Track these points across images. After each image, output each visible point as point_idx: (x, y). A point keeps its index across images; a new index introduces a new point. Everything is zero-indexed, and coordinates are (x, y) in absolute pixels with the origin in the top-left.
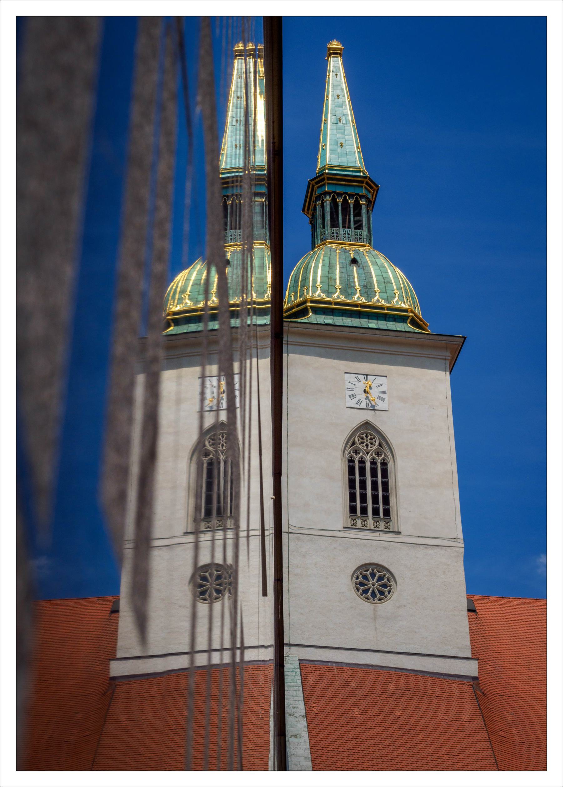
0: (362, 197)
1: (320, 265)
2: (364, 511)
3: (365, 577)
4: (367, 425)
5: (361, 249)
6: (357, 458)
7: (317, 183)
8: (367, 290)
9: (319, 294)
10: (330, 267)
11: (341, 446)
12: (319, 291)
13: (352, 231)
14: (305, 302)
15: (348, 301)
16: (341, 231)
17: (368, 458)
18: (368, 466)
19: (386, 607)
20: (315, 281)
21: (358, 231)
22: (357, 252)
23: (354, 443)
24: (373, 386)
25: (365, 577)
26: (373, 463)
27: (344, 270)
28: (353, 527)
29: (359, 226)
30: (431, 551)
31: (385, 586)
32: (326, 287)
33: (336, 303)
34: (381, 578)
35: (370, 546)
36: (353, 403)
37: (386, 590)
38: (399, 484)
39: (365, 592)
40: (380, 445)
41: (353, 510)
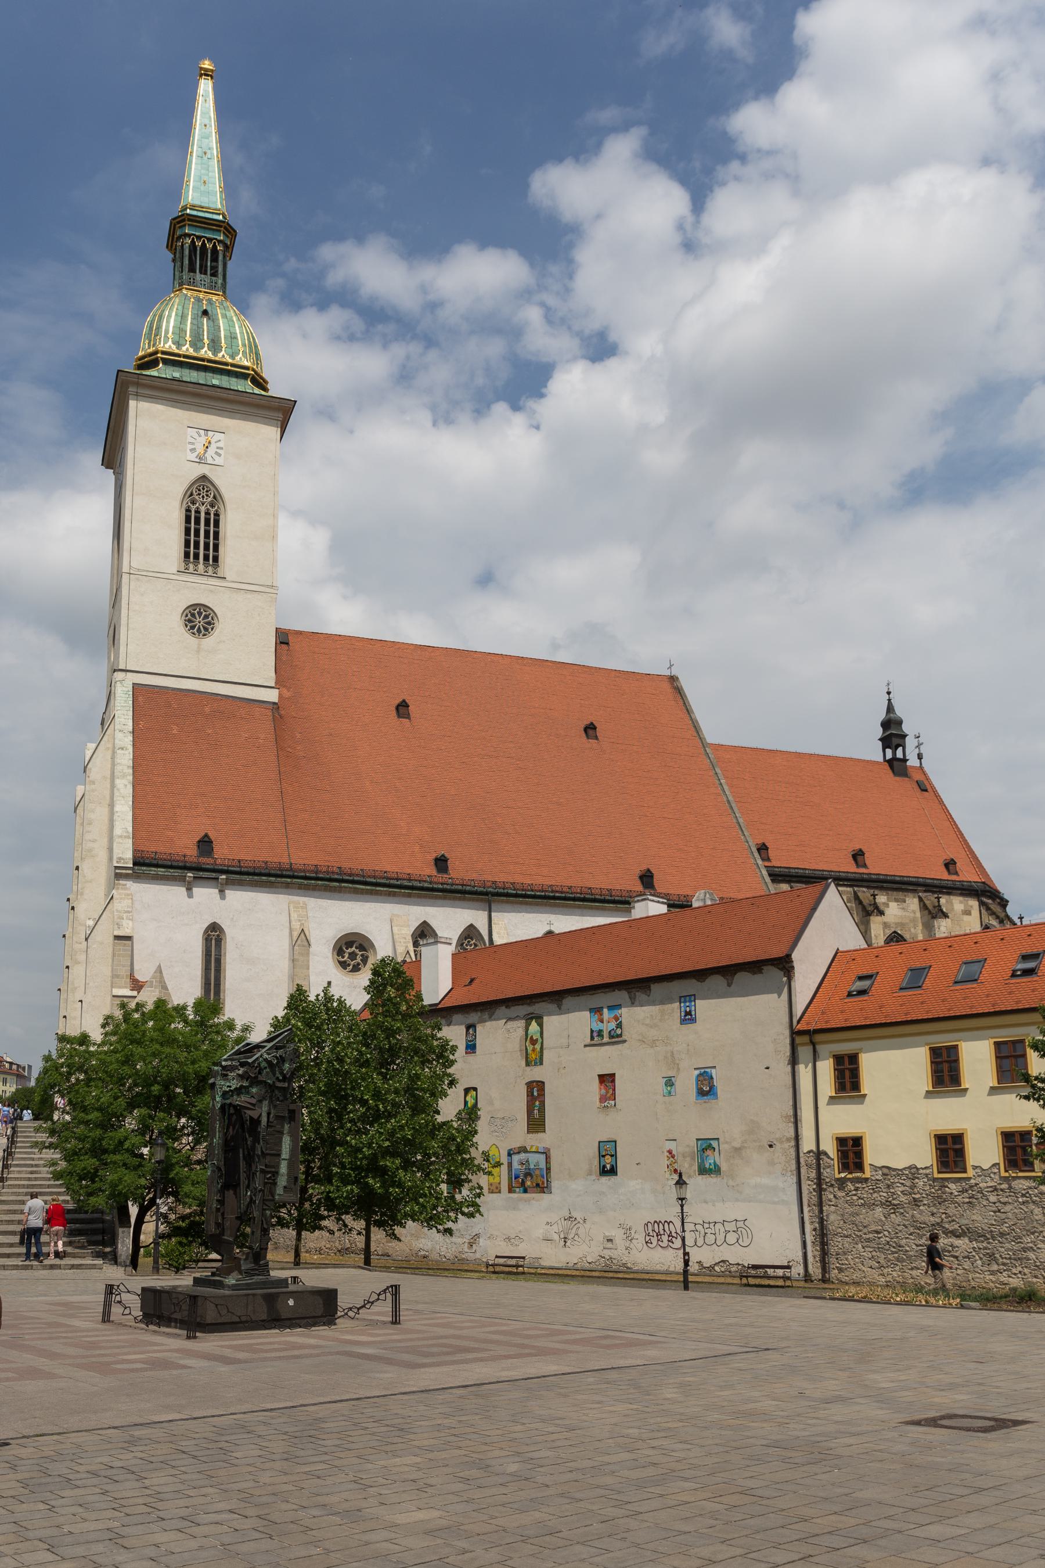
0: (220, 241)
1: (174, 314)
2: (196, 556)
3: (193, 615)
4: (204, 478)
5: (214, 298)
6: (193, 508)
7: (179, 223)
9: (169, 346)
10: (183, 317)
11: (180, 496)
12: (170, 343)
13: (207, 278)
14: (156, 353)
15: (195, 355)
16: (198, 276)
17: (203, 509)
18: (203, 515)
19: (209, 642)
20: (167, 332)
21: (214, 278)
22: (210, 301)
23: (192, 494)
24: (213, 441)
25: (193, 615)
26: (207, 513)
27: (195, 322)
28: (185, 571)
29: (214, 274)
30: (249, 596)
31: (209, 623)
32: (177, 338)
33: (185, 356)
34: (206, 617)
35: (199, 589)
38: (228, 534)
39: (193, 628)
40: (214, 497)
41: (187, 555)
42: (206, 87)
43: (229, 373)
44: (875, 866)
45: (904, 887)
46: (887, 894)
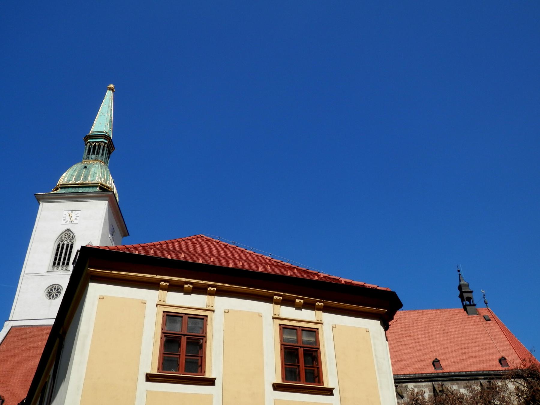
0: (102, 142)
2: (59, 264)
3: (52, 290)
8: (86, 178)
13: (94, 156)
25: (52, 290)
26: (68, 245)
28: (53, 271)
32: (69, 179)
34: (58, 289)
36: (64, 222)
37: (58, 294)
39: (50, 296)
40: (73, 238)
41: (54, 264)
42: (109, 94)
43: (89, 187)
44: (448, 367)
45: (468, 378)
46: (458, 384)
